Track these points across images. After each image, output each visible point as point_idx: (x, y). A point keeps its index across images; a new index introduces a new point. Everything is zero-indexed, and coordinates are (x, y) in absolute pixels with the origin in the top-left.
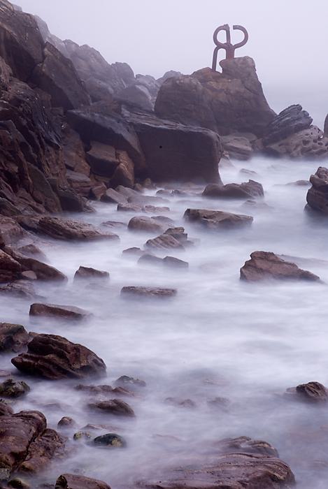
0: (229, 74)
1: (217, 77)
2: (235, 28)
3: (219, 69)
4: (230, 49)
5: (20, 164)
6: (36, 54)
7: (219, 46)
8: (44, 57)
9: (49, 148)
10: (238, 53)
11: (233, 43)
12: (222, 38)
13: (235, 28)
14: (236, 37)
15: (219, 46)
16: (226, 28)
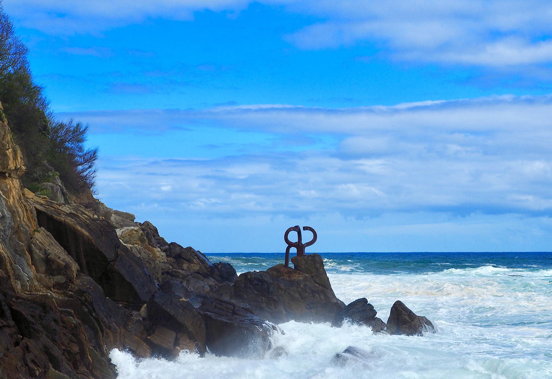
0: (301, 271)
1: (290, 272)
2: (305, 228)
3: (291, 265)
4: (300, 246)
5: (80, 343)
6: (110, 255)
7: (290, 245)
8: (117, 256)
9: (108, 331)
10: (308, 250)
11: (304, 242)
12: (293, 237)
13: (305, 228)
14: (307, 236)
15: (290, 245)
16: (296, 228)
